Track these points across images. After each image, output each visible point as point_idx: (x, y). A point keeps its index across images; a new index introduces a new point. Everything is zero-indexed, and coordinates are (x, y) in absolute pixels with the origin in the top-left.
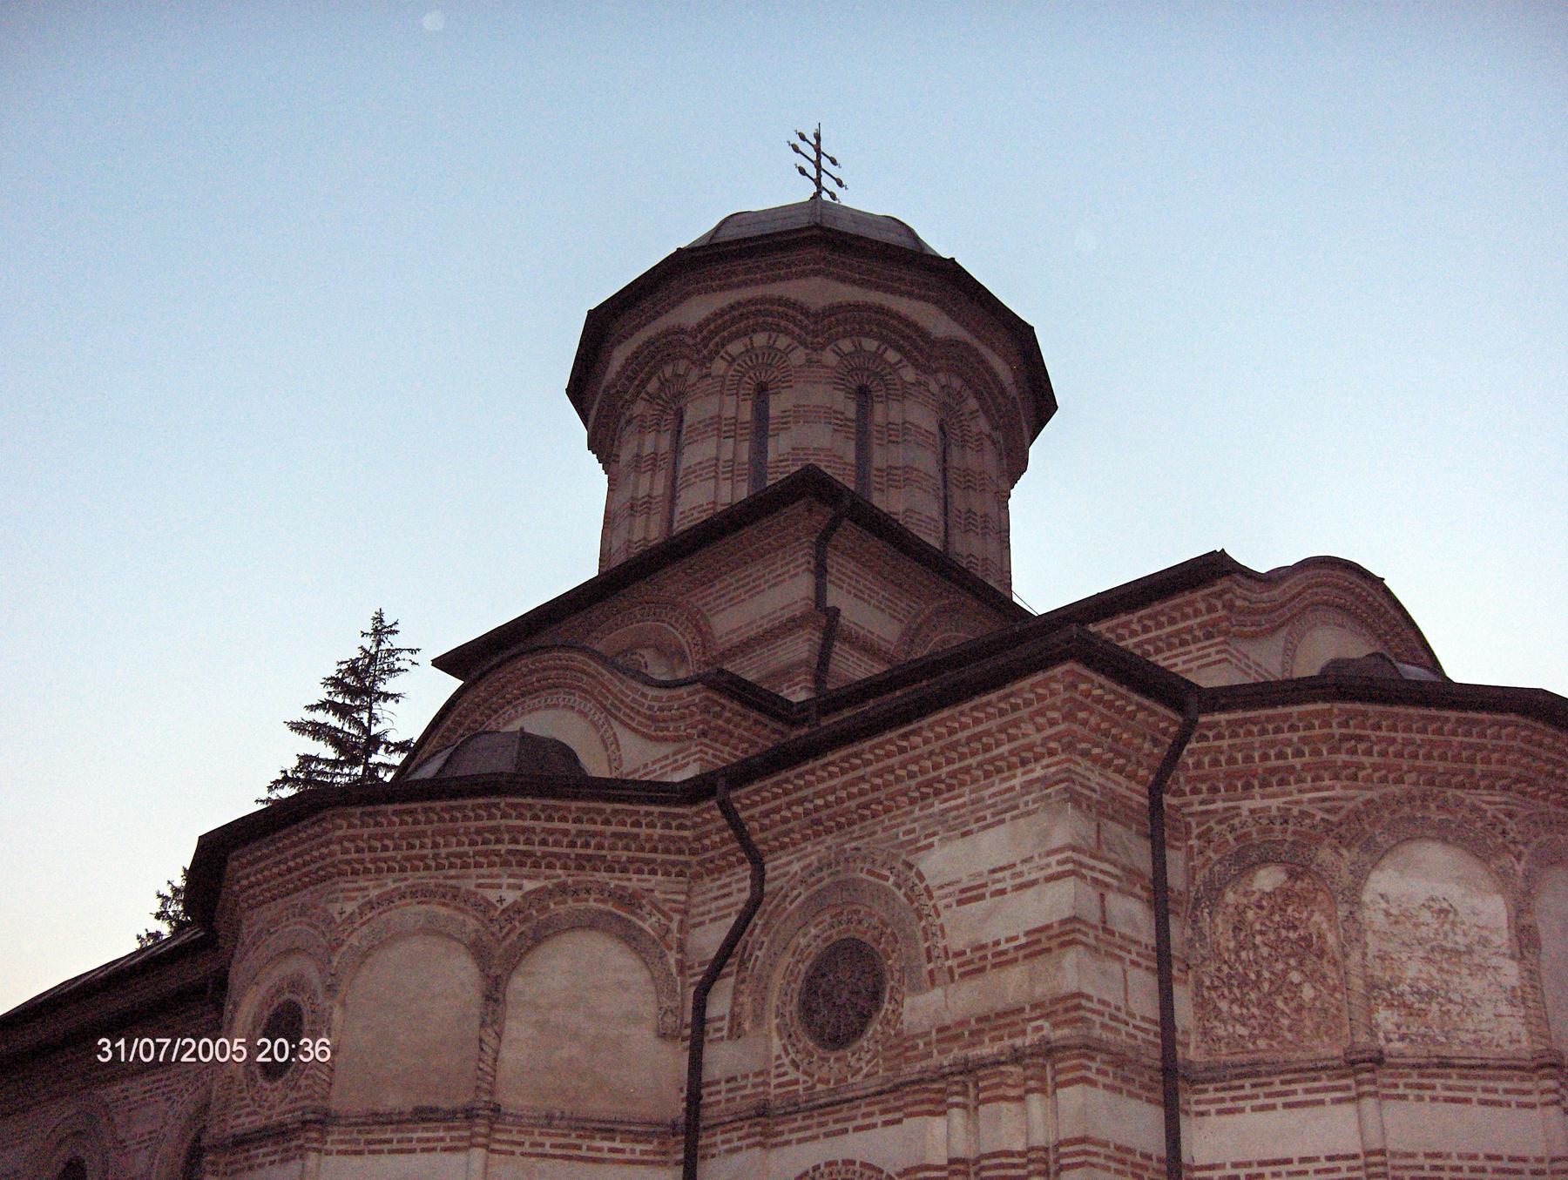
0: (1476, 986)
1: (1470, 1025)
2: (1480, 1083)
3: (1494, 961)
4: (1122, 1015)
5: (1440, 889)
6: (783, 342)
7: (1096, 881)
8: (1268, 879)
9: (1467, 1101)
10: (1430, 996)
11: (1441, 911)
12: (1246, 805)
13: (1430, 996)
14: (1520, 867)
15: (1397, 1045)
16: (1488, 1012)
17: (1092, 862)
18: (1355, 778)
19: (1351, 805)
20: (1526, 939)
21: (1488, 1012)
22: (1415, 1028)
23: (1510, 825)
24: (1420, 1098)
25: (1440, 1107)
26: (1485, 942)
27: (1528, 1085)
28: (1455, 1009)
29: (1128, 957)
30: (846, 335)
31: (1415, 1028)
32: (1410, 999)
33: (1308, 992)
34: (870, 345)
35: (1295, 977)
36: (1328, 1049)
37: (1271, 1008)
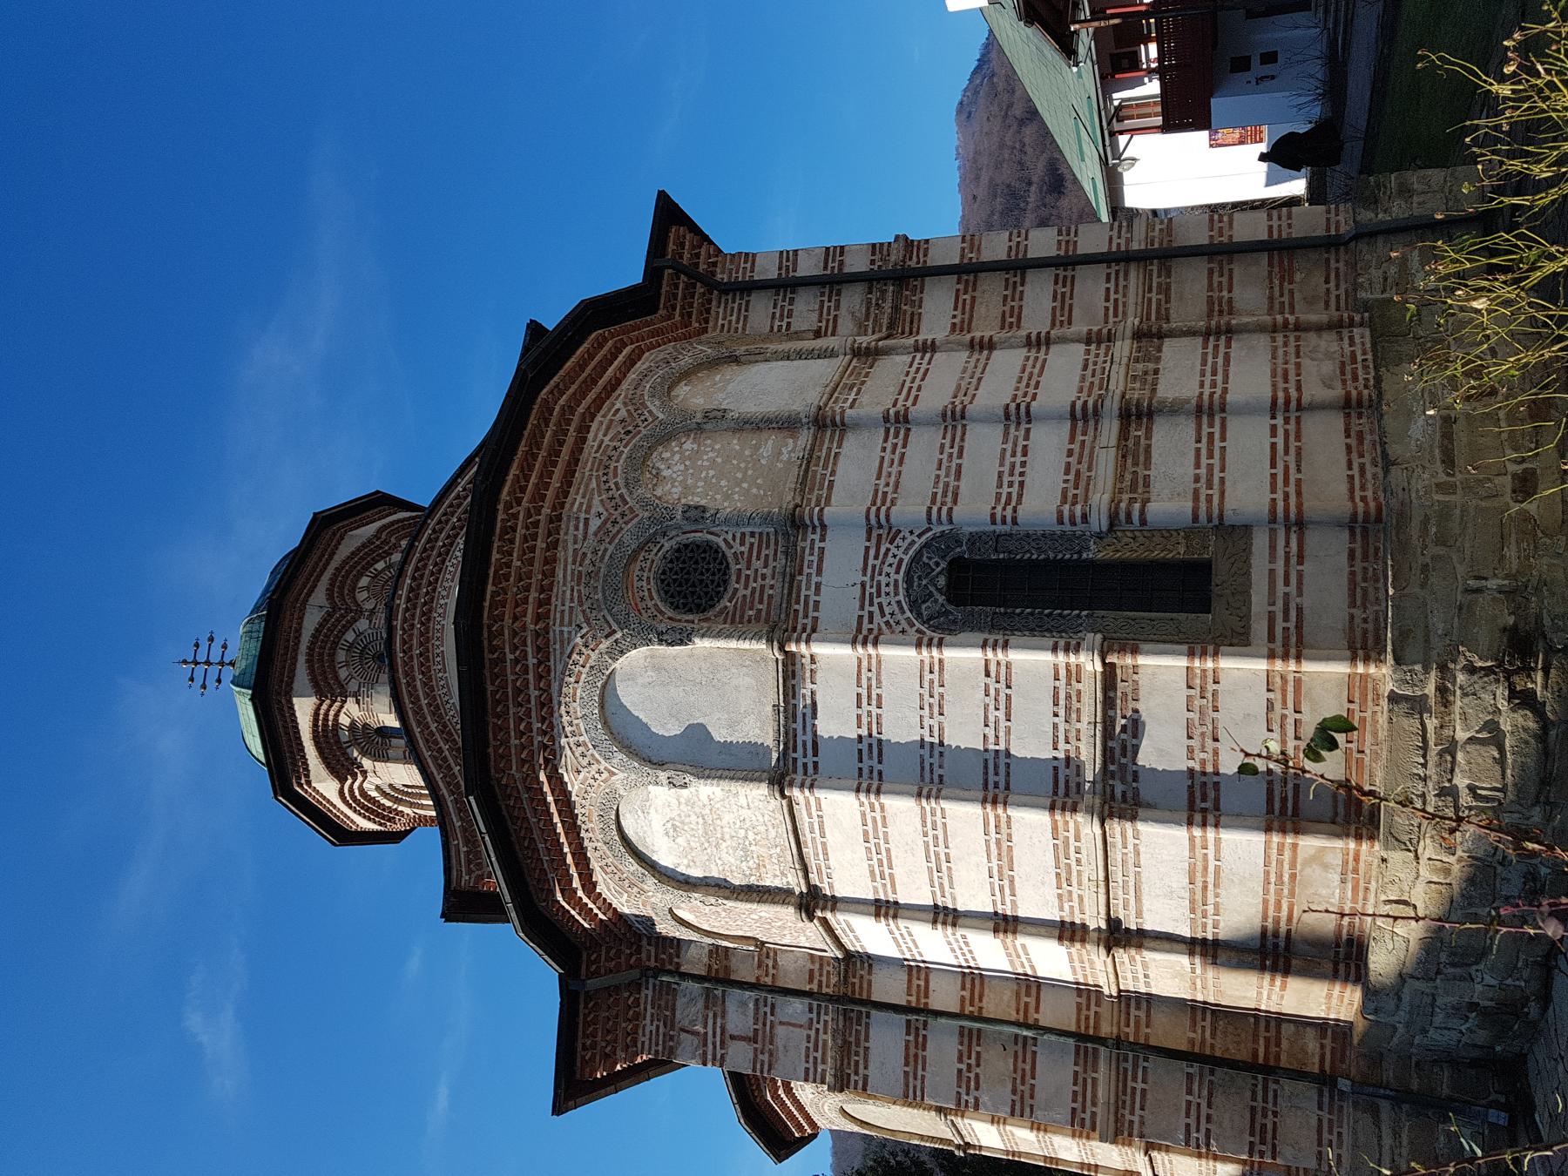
0: (727, 818)
1: (762, 829)
2: (809, 836)
4: (813, 1033)
7: (723, 1042)
9: (824, 844)
10: (745, 850)
11: (675, 827)
13: (745, 850)
16: (745, 813)
17: (710, 1047)
19: (612, 885)
21: (745, 813)
25: (832, 862)
28: (751, 836)
29: (769, 1018)
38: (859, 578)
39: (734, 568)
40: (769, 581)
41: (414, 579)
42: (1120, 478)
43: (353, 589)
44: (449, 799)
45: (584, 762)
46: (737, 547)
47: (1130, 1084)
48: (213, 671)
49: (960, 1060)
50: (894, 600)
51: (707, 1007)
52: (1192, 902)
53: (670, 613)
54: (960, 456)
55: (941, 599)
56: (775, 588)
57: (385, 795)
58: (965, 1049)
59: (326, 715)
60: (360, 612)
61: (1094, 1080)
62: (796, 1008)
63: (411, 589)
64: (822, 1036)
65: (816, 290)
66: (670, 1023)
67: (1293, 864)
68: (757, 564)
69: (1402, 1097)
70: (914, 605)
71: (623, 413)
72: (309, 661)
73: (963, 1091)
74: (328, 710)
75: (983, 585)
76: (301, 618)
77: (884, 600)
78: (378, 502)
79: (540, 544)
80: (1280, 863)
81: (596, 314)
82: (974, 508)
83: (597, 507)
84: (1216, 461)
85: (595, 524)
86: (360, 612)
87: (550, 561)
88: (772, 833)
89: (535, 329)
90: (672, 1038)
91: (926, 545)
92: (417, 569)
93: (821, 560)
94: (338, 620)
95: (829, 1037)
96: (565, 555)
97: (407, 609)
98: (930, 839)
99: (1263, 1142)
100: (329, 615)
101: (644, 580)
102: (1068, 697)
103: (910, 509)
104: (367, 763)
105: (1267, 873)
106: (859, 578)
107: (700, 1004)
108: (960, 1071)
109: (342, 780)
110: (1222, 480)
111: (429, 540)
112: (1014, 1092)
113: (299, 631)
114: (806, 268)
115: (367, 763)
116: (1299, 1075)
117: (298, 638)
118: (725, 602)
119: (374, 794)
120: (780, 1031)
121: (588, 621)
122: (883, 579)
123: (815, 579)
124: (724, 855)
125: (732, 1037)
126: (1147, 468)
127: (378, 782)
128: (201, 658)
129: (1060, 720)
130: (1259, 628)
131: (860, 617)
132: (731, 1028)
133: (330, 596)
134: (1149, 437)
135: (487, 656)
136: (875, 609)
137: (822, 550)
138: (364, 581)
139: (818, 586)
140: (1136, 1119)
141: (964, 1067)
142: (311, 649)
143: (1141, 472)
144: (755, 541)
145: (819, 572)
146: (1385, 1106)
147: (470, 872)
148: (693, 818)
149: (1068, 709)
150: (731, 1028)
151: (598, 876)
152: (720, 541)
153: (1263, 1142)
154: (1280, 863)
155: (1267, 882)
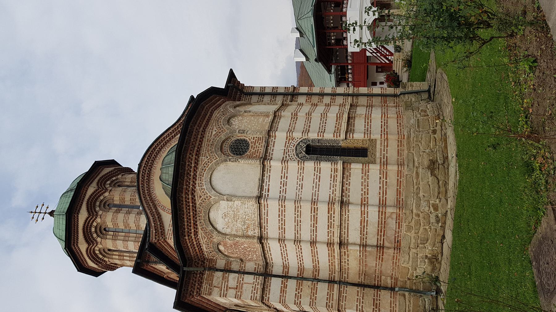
0: (241, 212)
2: (263, 216)
3: (235, 206)
4: (254, 285)
5: (220, 216)
6: (97, 248)
7: (227, 290)
8: (221, 248)
11: (225, 215)
12: (205, 250)
14: (213, 197)
15: (256, 231)
18: (197, 232)
19: (203, 234)
20: (230, 198)
22: (252, 227)
23: (202, 197)
24: (267, 229)
25: (268, 225)
26: (231, 207)
27: (263, 205)
29: (242, 282)
30: (92, 236)
31: (252, 227)
32: (245, 227)
33: (246, 245)
34: (93, 230)
35: (242, 247)
36: (259, 246)
37: (250, 251)
38: (284, 148)
39: (251, 145)
40: (260, 148)
41: (148, 159)
42: (347, 129)
43: (105, 184)
44: (151, 218)
45: (203, 194)
46: (252, 140)
47: (342, 294)
48: (42, 215)
49: (296, 291)
50: (292, 153)
51: (223, 279)
52: (361, 231)
53: (232, 155)
54: (310, 123)
55: (304, 153)
56: (262, 150)
57: (101, 253)
58: (298, 288)
59: (89, 221)
60: (107, 189)
61: (333, 294)
62: (249, 279)
63: (147, 161)
64: (257, 286)
65: (270, 96)
66: (211, 285)
67: (385, 219)
68: (257, 144)
69: (411, 291)
70: (297, 155)
71: (222, 110)
72: (87, 204)
73: (296, 299)
74: (90, 220)
75: (315, 151)
76: (87, 191)
77: (290, 153)
78: (112, 163)
79: (199, 137)
80: (382, 218)
81: (212, 92)
82: (313, 136)
83: (215, 129)
84: (369, 127)
85: (214, 133)
86: (107, 189)
87: (201, 141)
88: (253, 216)
89: (192, 97)
90: (211, 289)
91: (301, 141)
92: (149, 156)
93: (274, 144)
94: (99, 193)
95: (259, 286)
96: (205, 140)
97: (144, 167)
98: (296, 216)
99: (376, 308)
100: (96, 191)
101: (226, 148)
102: (334, 176)
103: (298, 135)
104: (99, 239)
105: (379, 221)
106: (284, 148)
107: (221, 279)
108: (296, 294)
109: (89, 245)
110: (367, 212)
111: (154, 149)
112: (311, 299)
113: (85, 195)
114: (267, 91)
115: (99, 239)
116: (386, 288)
117: (84, 197)
118: (248, 153)
119: (97, 252)
120: (244, 285)
121: (209, 156)
122: (290, 149)
123: (272, 148)
124: (238, 225)
125: (230, 288)
126: (354, 126)
127: (100, 246)
128: (38, 210)
129: (332, 182)
130: (378, 161)
131: (283, 157)
132: (230, 286)
133: (98, 185)
134: (354, 121)
135: (181, 162)
136: (287, 155)
137: (274, 142)
138: (108, 182)
139: (273, 150)
140: (343, 304)
141: (297, 293)
142: (88, 200)
143: (352, 128)
144: (257, 139)
145: (273, 146)
146: (407, 294)
147: (156, 238)
148: (231, 212)
149: (334, 179)
150: (230, 286)
151: (200, 231)
152: (247, 139)
153: (376, 308)
154: (382, 218)
155: (379, 224)
